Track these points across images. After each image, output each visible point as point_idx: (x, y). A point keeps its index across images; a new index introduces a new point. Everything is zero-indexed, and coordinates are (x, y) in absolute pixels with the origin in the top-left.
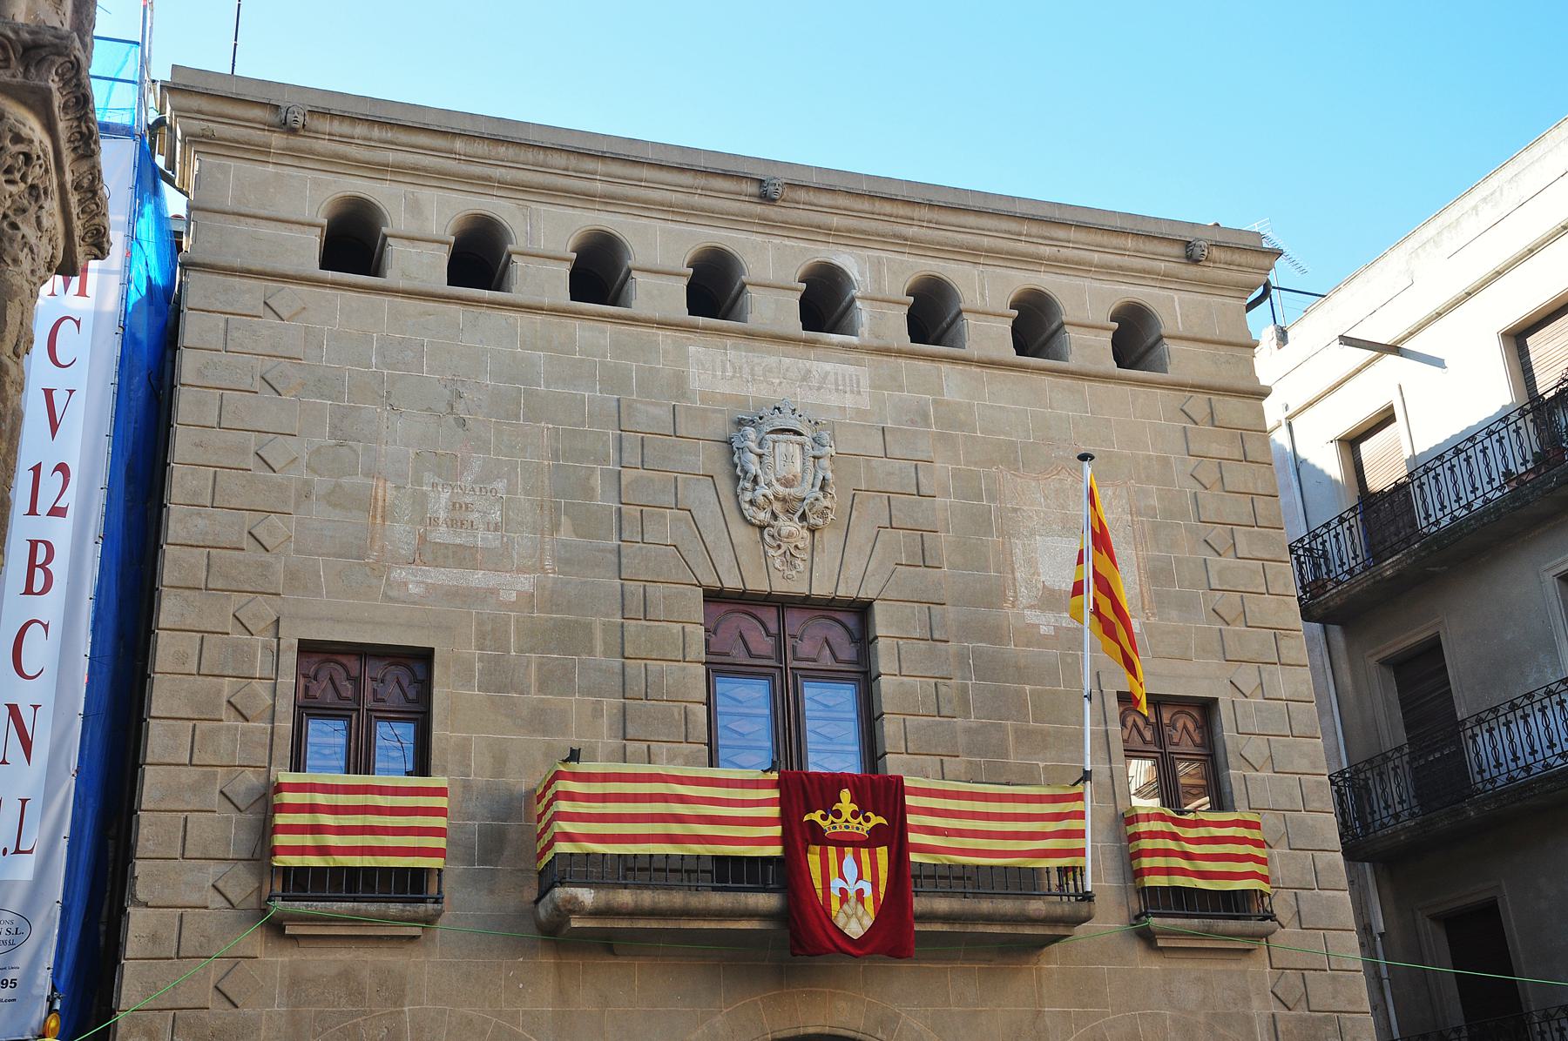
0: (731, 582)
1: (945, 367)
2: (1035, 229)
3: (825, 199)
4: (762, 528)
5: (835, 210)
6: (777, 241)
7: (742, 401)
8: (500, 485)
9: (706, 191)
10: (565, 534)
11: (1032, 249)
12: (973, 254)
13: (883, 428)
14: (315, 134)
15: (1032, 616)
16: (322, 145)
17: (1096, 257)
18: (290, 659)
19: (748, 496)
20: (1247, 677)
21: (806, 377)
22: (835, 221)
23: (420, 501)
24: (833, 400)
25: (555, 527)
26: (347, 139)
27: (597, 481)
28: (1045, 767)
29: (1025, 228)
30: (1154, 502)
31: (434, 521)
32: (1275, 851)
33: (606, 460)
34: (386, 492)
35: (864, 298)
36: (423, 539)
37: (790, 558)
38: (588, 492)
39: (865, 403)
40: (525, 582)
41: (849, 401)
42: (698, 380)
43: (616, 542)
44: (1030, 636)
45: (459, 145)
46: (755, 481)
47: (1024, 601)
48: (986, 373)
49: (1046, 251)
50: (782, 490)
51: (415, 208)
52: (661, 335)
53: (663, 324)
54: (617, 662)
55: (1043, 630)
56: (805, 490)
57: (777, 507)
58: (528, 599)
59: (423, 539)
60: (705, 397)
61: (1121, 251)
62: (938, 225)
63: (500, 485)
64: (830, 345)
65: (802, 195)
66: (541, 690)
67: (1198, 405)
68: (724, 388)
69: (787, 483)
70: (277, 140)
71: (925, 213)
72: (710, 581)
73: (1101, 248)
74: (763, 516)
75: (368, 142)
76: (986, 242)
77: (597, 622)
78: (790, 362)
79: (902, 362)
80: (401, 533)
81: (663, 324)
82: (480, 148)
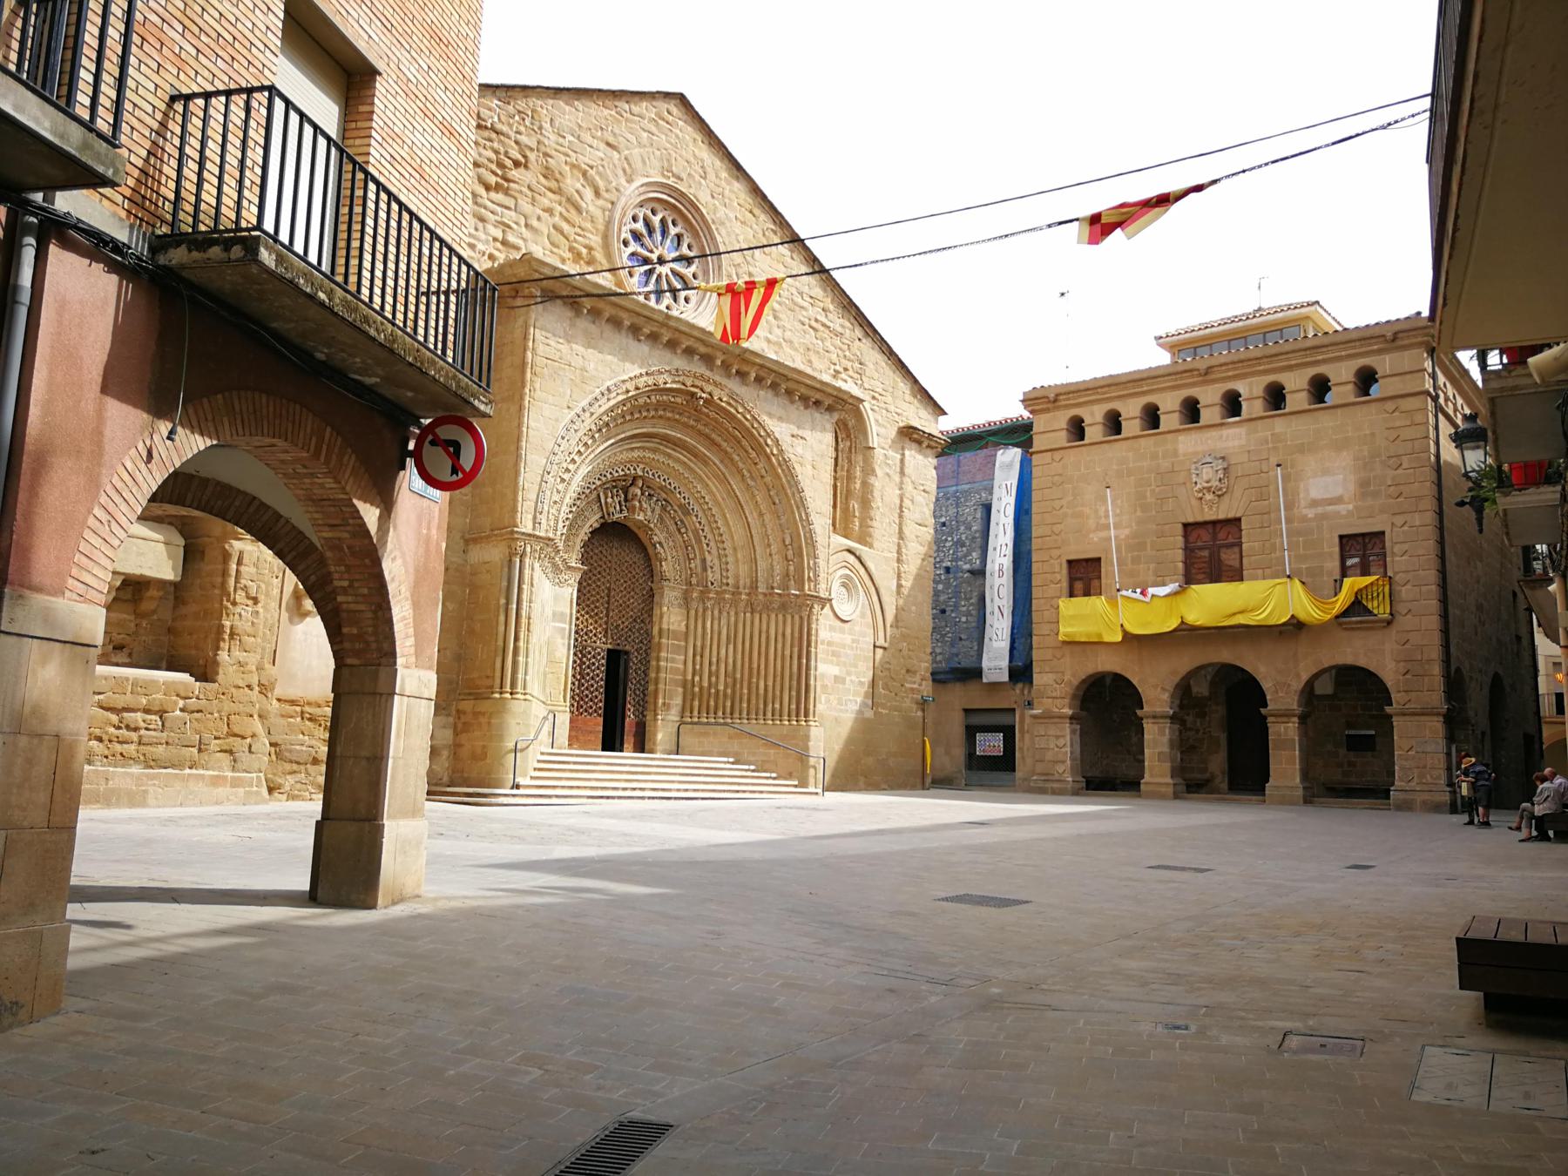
0: (1191, 520)
1: (1276, 419)
2: (1313, 351)
3: (1224, 368)
4: (1201, 499)
5: (1229, 370)
6: (1211, 387)
7: (1196, 453)
8: (1119, 501)
9: (1181, 379)
10: (1139, 513)
11: (1313, 359)
12: (1290, 368)
13: (1249, 452)
14: (1060, 401)
15: (1305, 511)
16: (1063, 403)
17: (1343, 353)
18: (1065, 565)
19: (1196, 488)
20: (1399, 520)
21: (1221, 437)
22: (1230, 374)
23: (1096, 511)
24: (1230, 444)
25: (1135, 511)
26: (1068, 399)
27: (1148, 494)
28: (1306, 568)
29: (1308, 352)
30: (1366, 453)
31: (1101, 517)
32: (1403, 588)
33: (1150, 485)
34: (1087, 510)
35: (1244, 400)
36: (1098, 523)
37: (1211, 508)
38: (1145, 498)
39: (1243, 442)
40: (1127, 531)
41: (1236, 443)
42: (1182, 448)
43: (1154, 513)
44: (1304, 519)
45: (1099, 390)
46: (1196, 483)
47: (1303, 503)
48: (1293, 417)
49: (1320, 358)
50: (1206, 485)
51: (1092, 414)
52: (1169, 436)
53: (1170, 432)
54: (1154, 552)
55: (1310, 516)
56: (1215, 483)
57: (1205, 491)
58: (1127, 537)
59: (1098, 523)
60: (1184, 456)
61: (1354, 348)
62: (1271, 362)
63: (1119, 501)
64: (1229, 423)
65: (1216, 369)
66: (1133, 563)
67: (1390, 406)
68: (1191, 450)
69: (1207, 482)
70: (1050, 405)
71: (1265, 360)
72: (1184, 521)
73: (1345, 349)
74: (1200, 495)
75: (1074, 398)
76: (1293, 362)
77: (1148, 541)
78: (1214, 433)
79: (1260, 422)
80: (1092, 523)
81: (1170, 432)
82: (1106, 389)
